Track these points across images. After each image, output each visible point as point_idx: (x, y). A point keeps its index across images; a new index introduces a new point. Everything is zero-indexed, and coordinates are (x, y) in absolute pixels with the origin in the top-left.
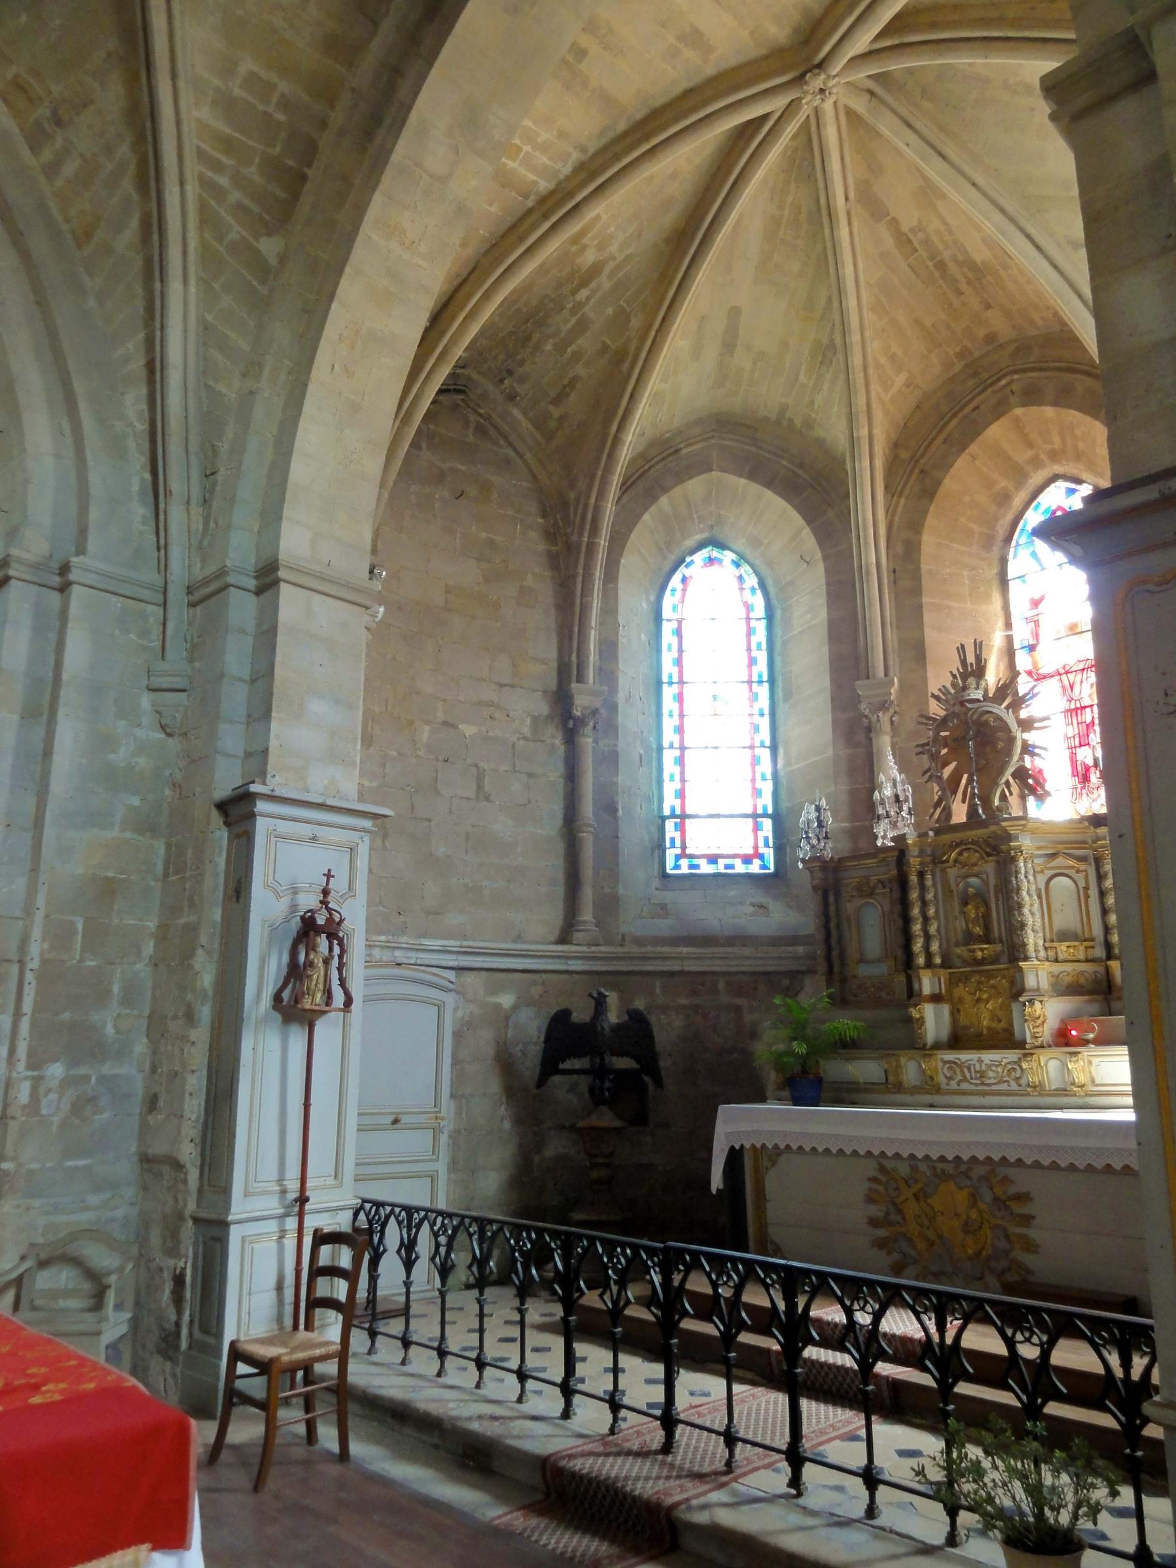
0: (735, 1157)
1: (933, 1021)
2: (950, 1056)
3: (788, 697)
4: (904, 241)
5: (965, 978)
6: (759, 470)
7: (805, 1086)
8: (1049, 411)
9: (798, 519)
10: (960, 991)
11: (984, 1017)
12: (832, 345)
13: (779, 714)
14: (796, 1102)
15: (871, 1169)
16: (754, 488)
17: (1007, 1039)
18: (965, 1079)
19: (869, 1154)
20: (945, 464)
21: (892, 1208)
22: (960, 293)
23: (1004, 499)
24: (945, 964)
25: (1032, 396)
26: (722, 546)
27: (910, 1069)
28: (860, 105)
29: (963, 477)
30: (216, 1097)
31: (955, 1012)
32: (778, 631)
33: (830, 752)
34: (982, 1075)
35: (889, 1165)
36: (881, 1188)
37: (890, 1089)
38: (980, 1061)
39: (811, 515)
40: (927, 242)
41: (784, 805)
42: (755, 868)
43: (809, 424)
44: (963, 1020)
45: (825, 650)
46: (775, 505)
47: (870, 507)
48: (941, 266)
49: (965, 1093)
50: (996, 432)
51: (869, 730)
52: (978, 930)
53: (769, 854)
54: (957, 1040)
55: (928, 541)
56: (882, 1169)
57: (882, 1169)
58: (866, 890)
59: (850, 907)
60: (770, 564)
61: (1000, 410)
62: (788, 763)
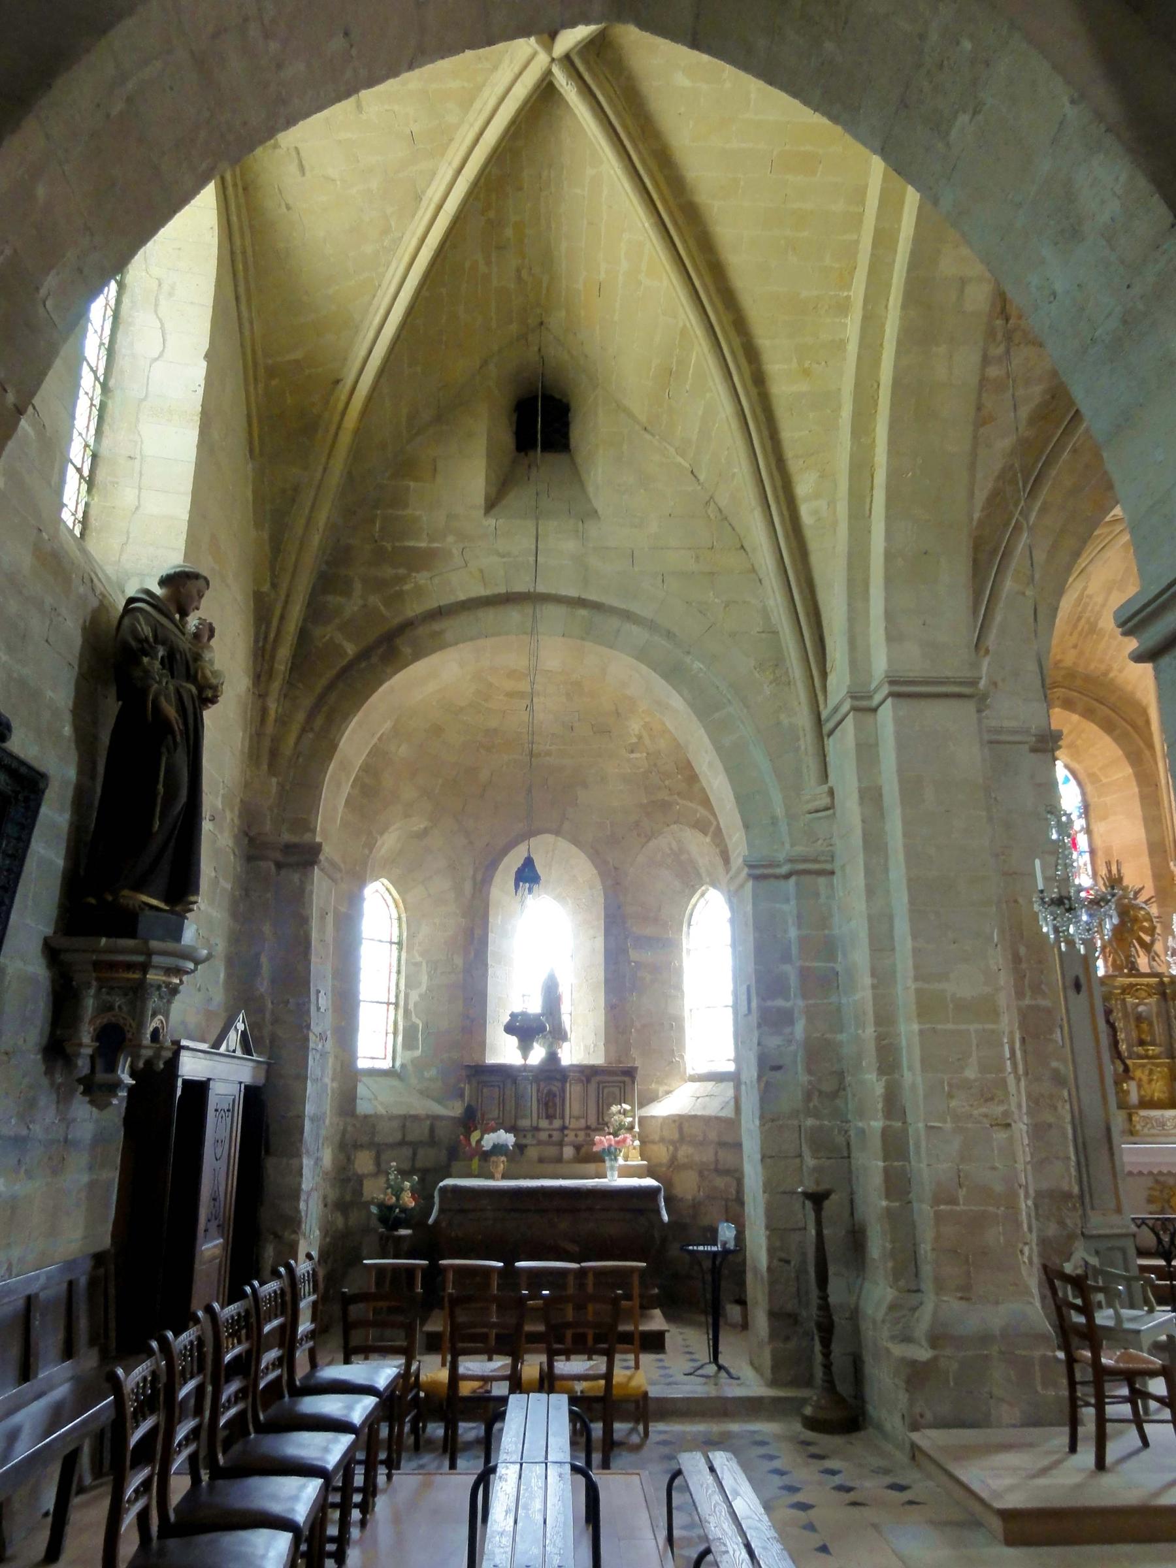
2: (1143, 1113)
15: (1150, 1182)
18: (1153, 1127)
19: (1140, 1173)
21: (1166, 1206)
22: (1071, 634)
30: (1084, 1144)
31: (1139, 1086)
34: (1163, 1125)
35: (1162, 1179)
36: (1157, 1193)
38: (1162, 1116)
40: (1087, 604)
44: (1143, 1093)
48: (1079, 619)
49: (1153, 1135)
56: (1157, 1182)
57: (1157, 1182)
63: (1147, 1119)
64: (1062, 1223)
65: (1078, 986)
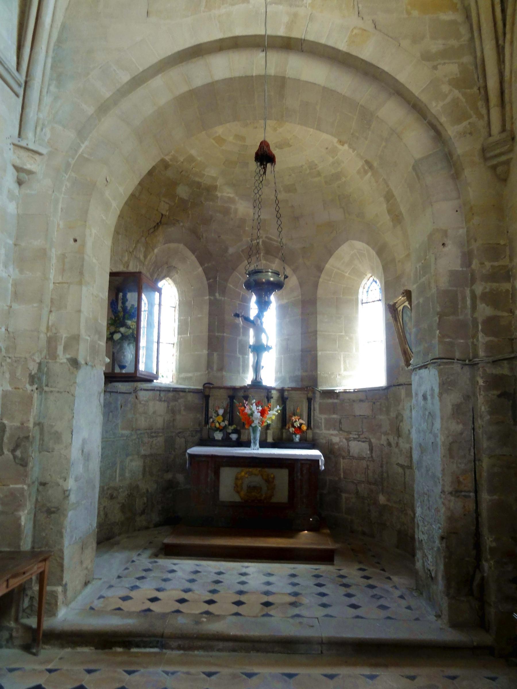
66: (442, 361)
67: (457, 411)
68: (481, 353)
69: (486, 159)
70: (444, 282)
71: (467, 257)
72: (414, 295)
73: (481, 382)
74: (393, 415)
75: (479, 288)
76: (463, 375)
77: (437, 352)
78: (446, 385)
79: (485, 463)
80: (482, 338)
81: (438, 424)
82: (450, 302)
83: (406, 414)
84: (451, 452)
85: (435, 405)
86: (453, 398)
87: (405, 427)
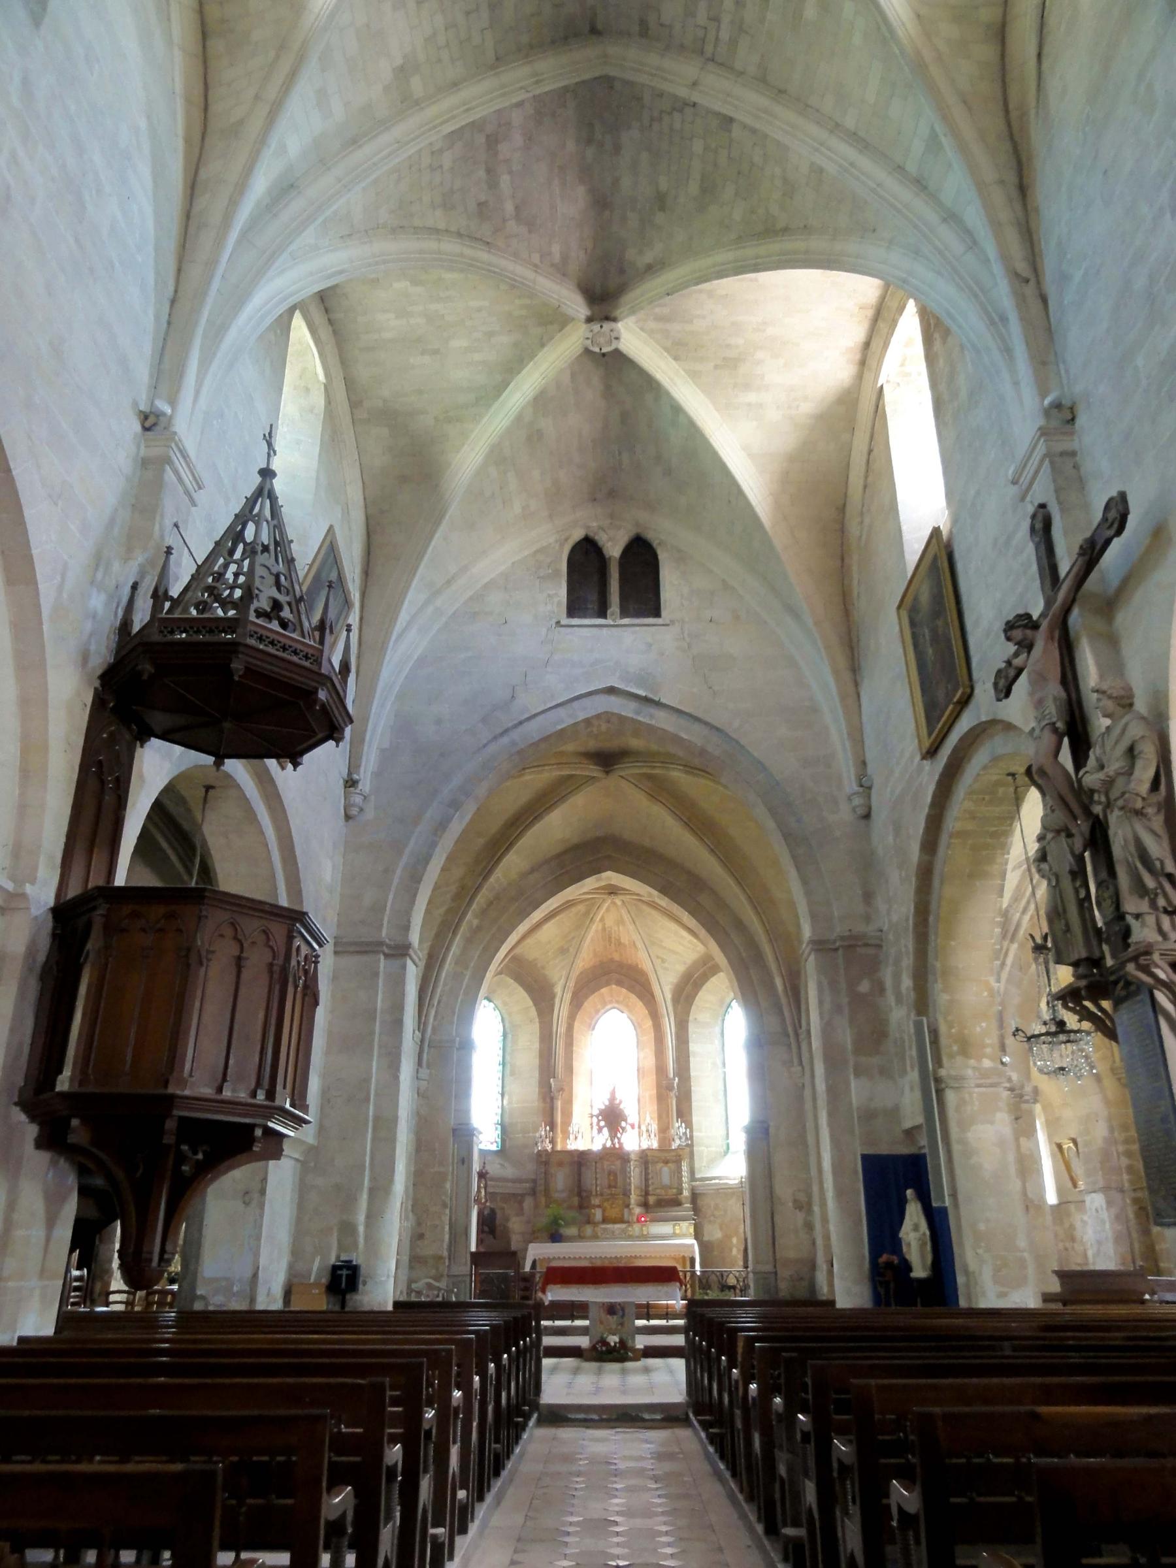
0: (534, 1262)
1: (598, 1214)
2: (603, 1226)
3: (512, 1074)
4: (604, 929)
5: (608, 1200)
6: (519, 979)
7: (555, 1237)
8: (624, 990)
9: (531, 1003)
10: (606, 1204)
11: (613, 1213)
12: (568, 950)
13: (508, 1080)
14: (553, 1242)
16: (516, 985)
17: (622, 1221)
20: (586, 997)
23: (597, 1011)
24: (602, 1195)
25: (619, 983)
26: (490, 1001)
27: (588, 1230)
28: (619, 903)
29: (589, 1004)
31: (604, 1211)
32: (509, 1044)
33: (536, 1104)
37: (581, 1237)
39: (536, 1003)
41: (507, 1120)
42: (494, 1148)
43: (543, 968)
45: (537, 1061)
46: (521, 993)
47: (562, 1009)
48: (610, 938)
50: (604, 990)
51: (552, 1099)
52: (613, 1184)
53: (499, 1140)
54: (605, 1220)
55: (576, 1025)
58: (560, 1164)
59: (553, 1170)
60: (510, 1014)
61: (608, 984)
62: (510, 1103)
63: (605, 1229)
64: (437, 1269)
65: (463, 1162)
66: (1106, 1189)
67: (1117, 1217)
68: (1127, 1185)
69: (1114, 1074)
70: (1099, 1143)
71: (1111, 1129)
72: (1079, 1140)
73: (1128, 1201)
74: (1067, 1225)
75: (1121, 1148)
76: (1117, 1196)
77: (1101, 1184)
78: (1109, 1203)
79: (1137, 1246)
80: (1125, 1177)
81: (1108, 1226)
82: (1106, 1155)
83: (1078, 1225)
84: (1117, 1239)
85: (1105, 1215)
86: (1114, 1211)
87: (1078, 1234)
